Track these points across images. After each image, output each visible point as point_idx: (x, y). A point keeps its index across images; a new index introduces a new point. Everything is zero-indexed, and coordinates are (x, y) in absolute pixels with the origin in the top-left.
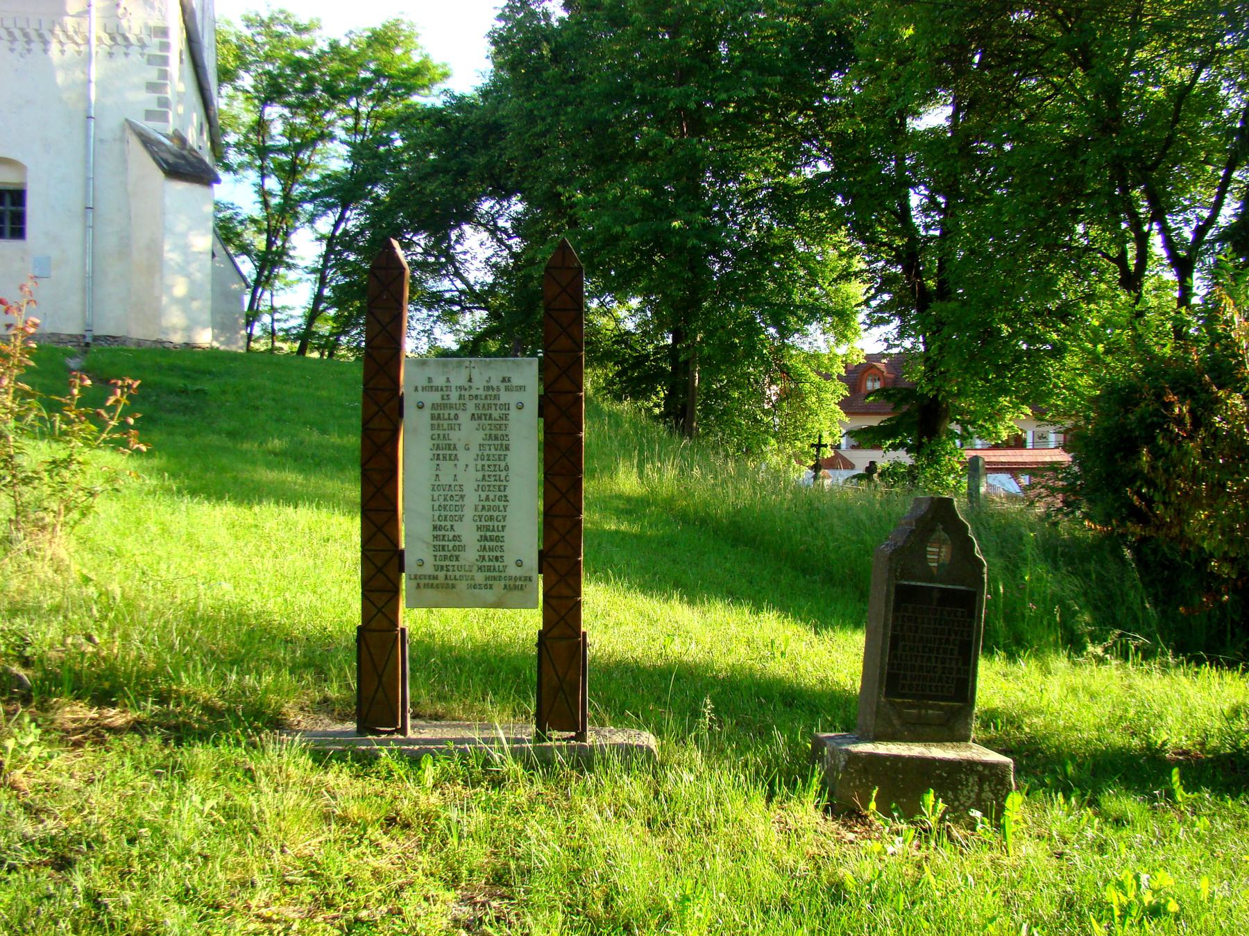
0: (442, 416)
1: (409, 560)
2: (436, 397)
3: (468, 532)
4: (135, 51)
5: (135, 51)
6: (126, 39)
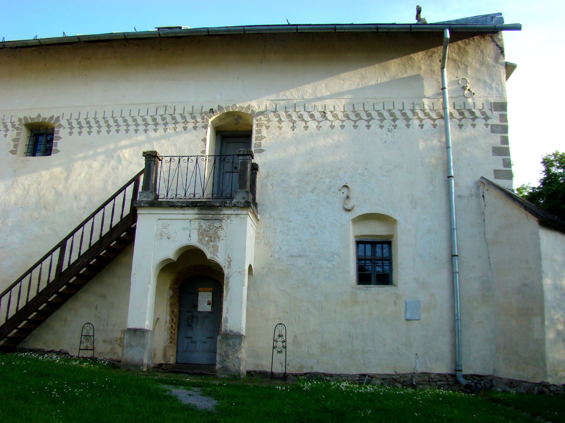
4: (480, 123)
5: (480, 123)
6: (472, 113)
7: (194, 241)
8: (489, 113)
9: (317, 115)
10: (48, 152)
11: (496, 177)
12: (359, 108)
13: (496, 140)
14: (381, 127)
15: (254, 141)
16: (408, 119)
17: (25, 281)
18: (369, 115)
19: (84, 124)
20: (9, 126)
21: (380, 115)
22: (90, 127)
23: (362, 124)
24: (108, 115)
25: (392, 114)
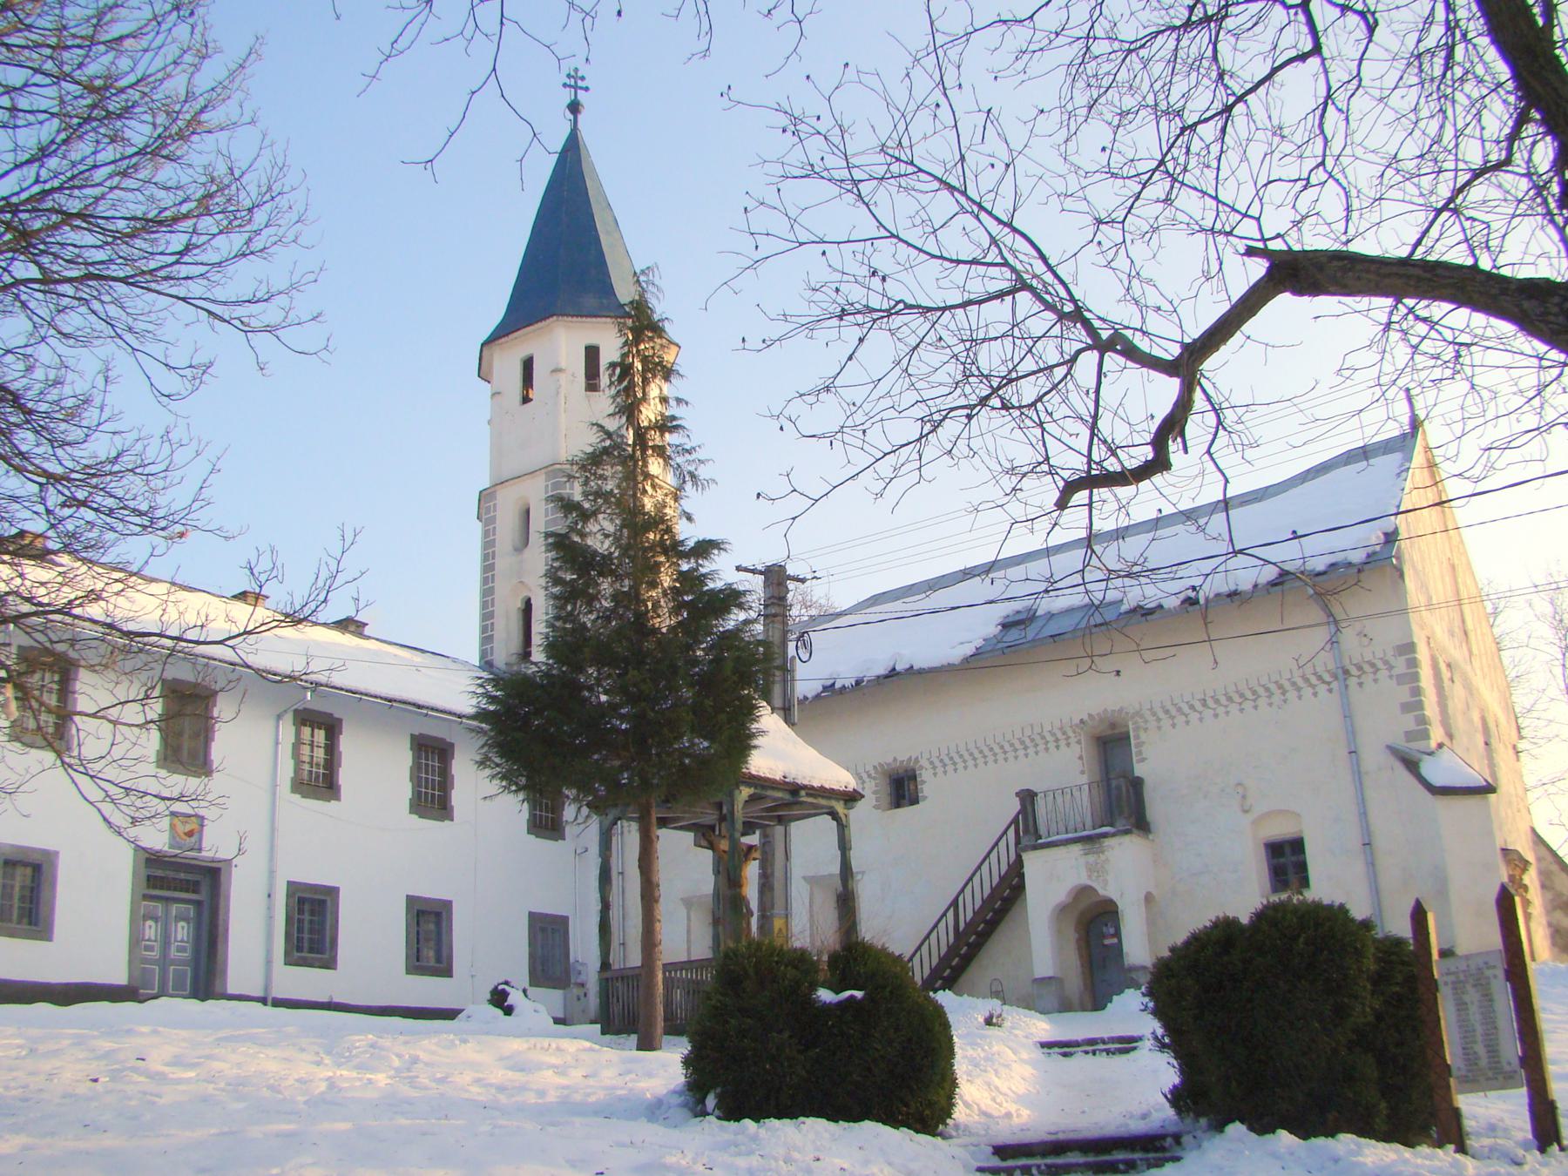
0: (1458, 987)
1: (1454, 1071)
2: (1452, 978)
3: (1480, 1049)
7: (1084, 880)
8: (1392, 661)
9: (1198, 706)
10: (914, 801)
11: (1408, 741)
12: (1242, 687)
13: (1404, 694)
14: (1270, 705)
15: (1134, 750)
16: (1299, 689)
17: (925, 948)
18: (1254, 692)
19: (947, 760)
20: (865, 776)
21: (1267, 690)
22: (955, 764)
23: (1248, 705)
24: (971, 746)
25: (1280, 687)
